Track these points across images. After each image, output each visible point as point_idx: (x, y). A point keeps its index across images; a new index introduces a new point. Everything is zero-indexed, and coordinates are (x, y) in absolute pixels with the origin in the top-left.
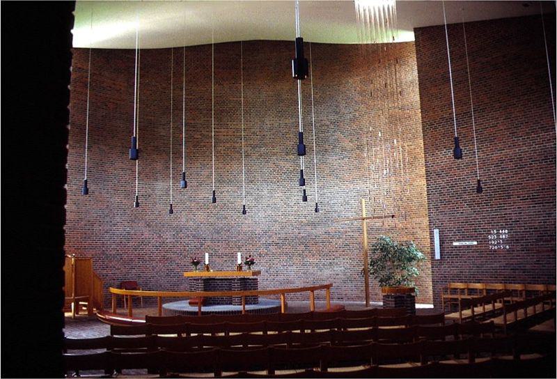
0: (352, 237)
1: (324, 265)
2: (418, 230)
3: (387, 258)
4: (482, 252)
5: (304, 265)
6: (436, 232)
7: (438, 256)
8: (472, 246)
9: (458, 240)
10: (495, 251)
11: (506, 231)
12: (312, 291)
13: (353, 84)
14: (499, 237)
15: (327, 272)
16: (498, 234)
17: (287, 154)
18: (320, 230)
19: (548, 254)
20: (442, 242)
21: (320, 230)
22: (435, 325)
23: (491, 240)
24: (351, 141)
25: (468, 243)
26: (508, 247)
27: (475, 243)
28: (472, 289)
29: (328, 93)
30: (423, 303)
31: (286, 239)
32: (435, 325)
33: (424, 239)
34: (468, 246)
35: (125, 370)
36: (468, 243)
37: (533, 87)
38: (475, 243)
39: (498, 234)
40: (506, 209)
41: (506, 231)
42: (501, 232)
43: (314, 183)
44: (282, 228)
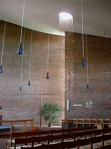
0: (31, 101)
1: (19, 111)
2: (56, 100)
3: (47, 111)
4: (84, 108)
5: (11, 110)
6: (68, 101)
7: (68, 109)
8: (80, 106)
9: (75, 104)
10: (87, 108)
11: (92, 102)
12: (25, 122)
13: (37, 45)
14: (89, 104)
15: (20, 114)
16: (89, 103)
17: (8, 66)
18: (18, 97)
19: (104, 109)
20: (69, 104)
21: (18, 97)
22: (79, 132)
23: (86, 104)
24: (34, 65)
25: (78, 105)
26: (92, 107)
27: (81, 105)
28: (79, 121)
29: (27, 46)
30: (57, 126)
31: (5, 100)
32: (79, 132)
33: (62, 102)
34: (79, 106)
35: (110, 134)
36: (78, 105)
37: (103, 58)
38: (81, 105)
39: (89, 103)
40: (92, 95)
41: (92, 102)
42: (90, 102)
43: (69, 80)
44: (3, 95)
